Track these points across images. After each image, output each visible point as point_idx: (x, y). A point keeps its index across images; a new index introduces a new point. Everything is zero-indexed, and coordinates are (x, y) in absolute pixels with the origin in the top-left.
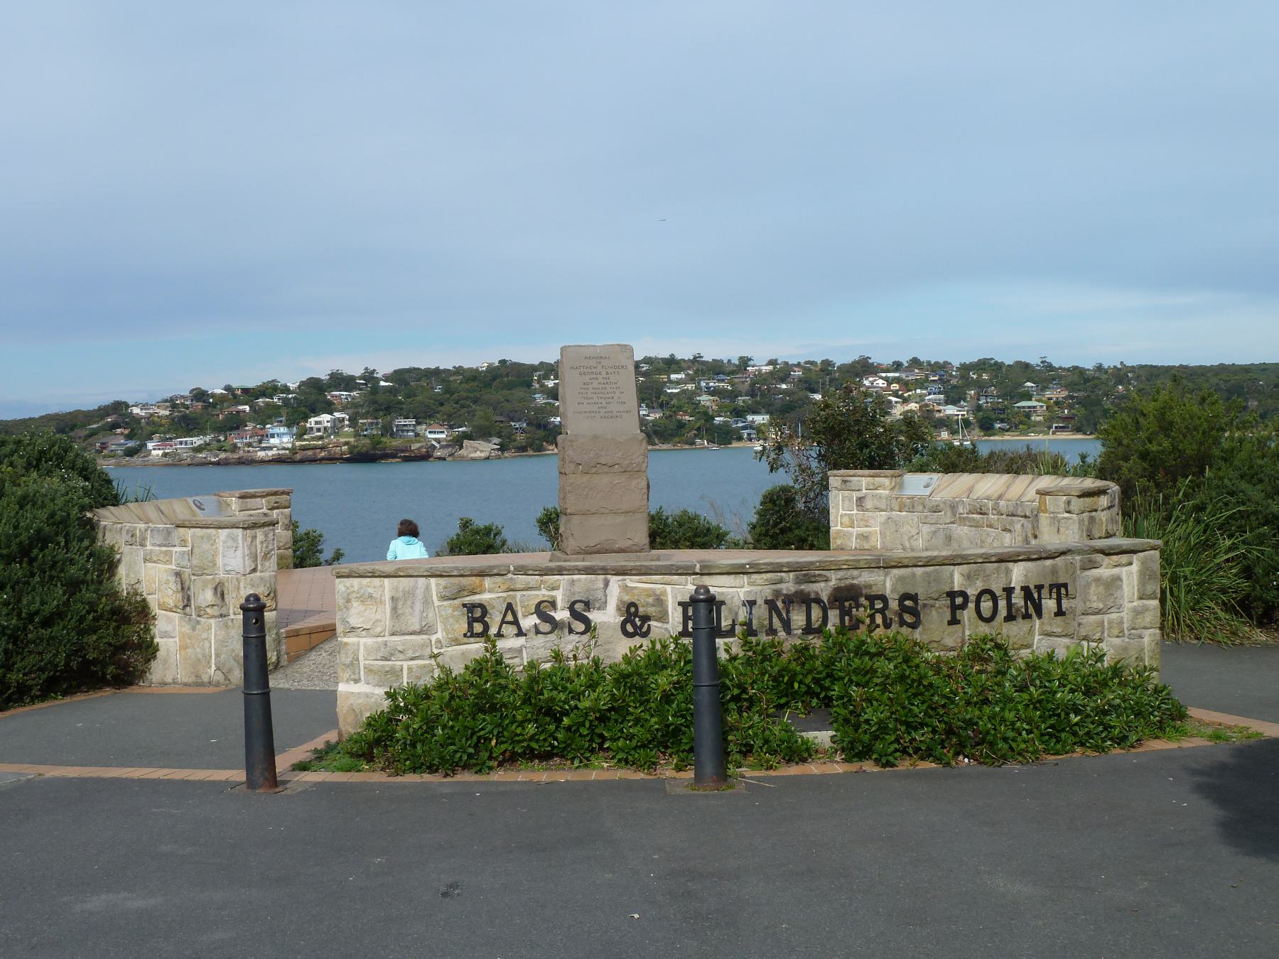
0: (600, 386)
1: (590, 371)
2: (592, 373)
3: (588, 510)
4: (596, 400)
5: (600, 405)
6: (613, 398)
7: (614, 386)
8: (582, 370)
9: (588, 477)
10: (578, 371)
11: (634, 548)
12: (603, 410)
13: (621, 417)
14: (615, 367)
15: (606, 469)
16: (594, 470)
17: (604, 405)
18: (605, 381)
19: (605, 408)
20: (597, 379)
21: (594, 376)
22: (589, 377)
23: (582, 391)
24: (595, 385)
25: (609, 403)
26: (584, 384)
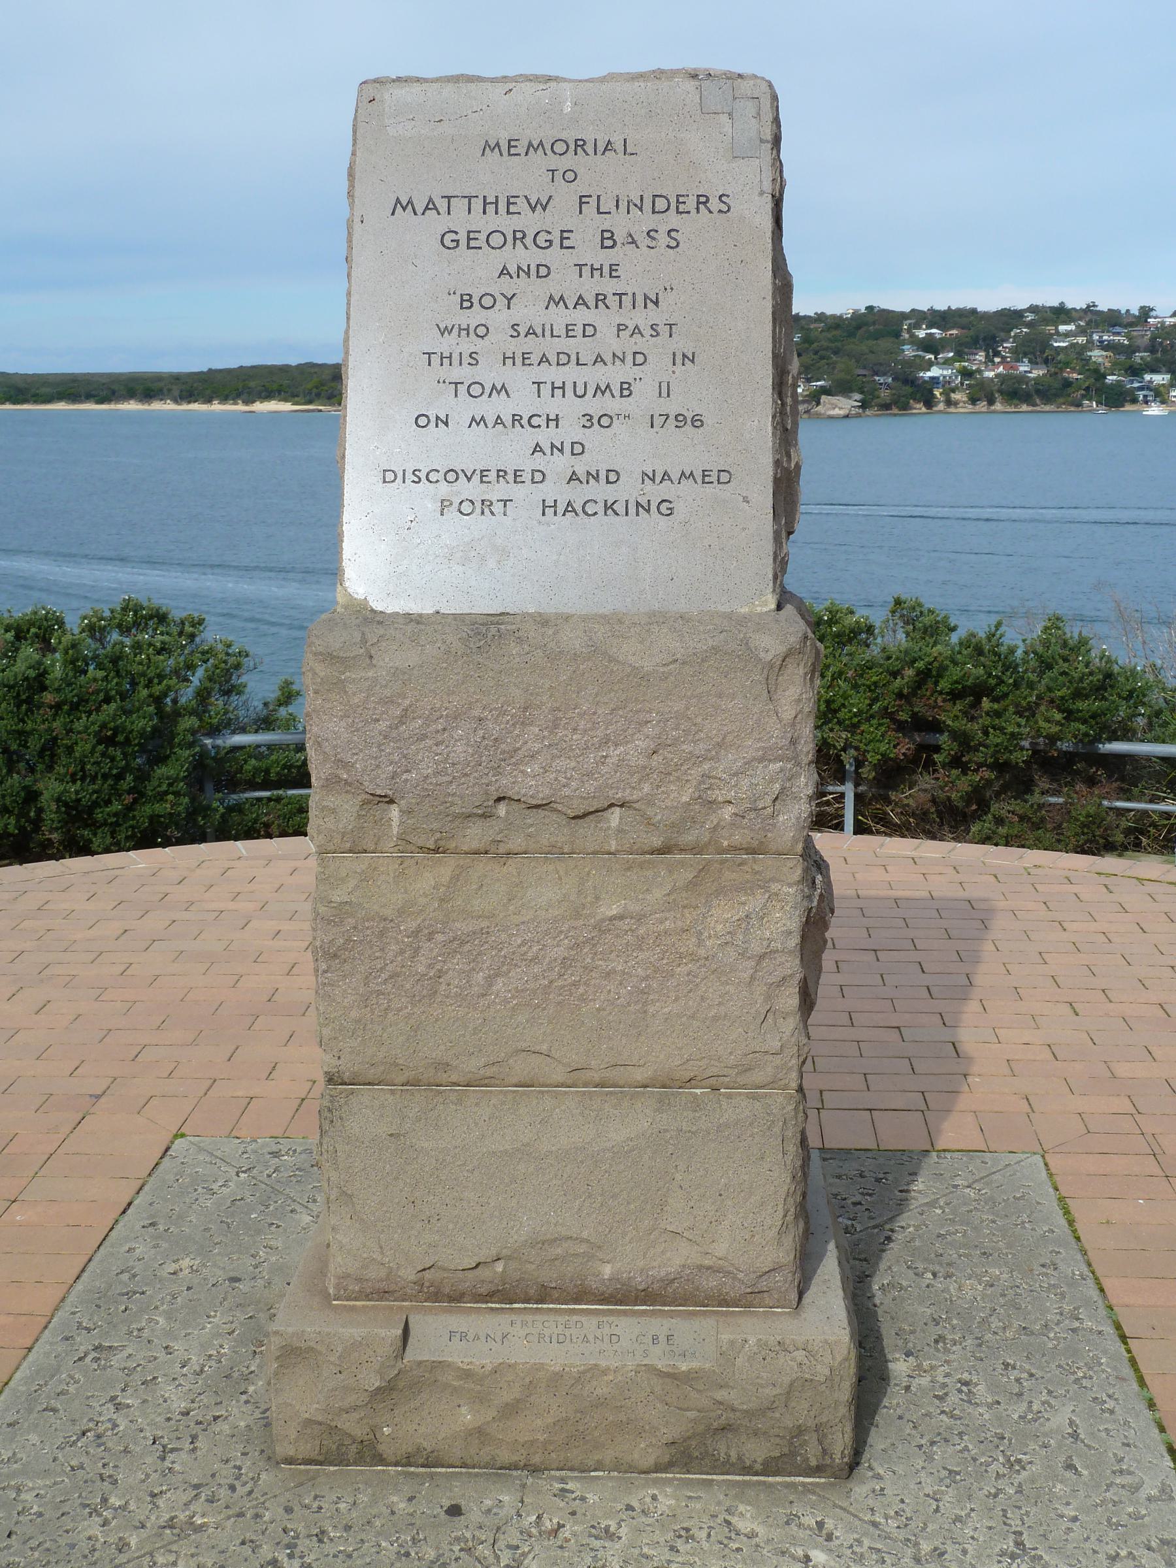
0: (559, 317)
1: (507, 224)
2: (519, 237)
3: (446, 1066)
4: (523, 402)
5: (545, 436)
6: (626, 390)
7: (642, 318)
8: (461, 220)
9: (446, 868)
10: (437, 223)
11: (710, 1283)
12: (560, 464)
13: (666, 508)
14: (657, 204)
15: (551, 830)
16: (475, 835)
17: (570, 432)
18: (589, 287)
19: (578, 449)
20: (543, 272)
21: (527, 256)
22: (496, 260)
23: (446, 344)
24: (529, 311)
25: (604, 421)
26: (466, 302)
